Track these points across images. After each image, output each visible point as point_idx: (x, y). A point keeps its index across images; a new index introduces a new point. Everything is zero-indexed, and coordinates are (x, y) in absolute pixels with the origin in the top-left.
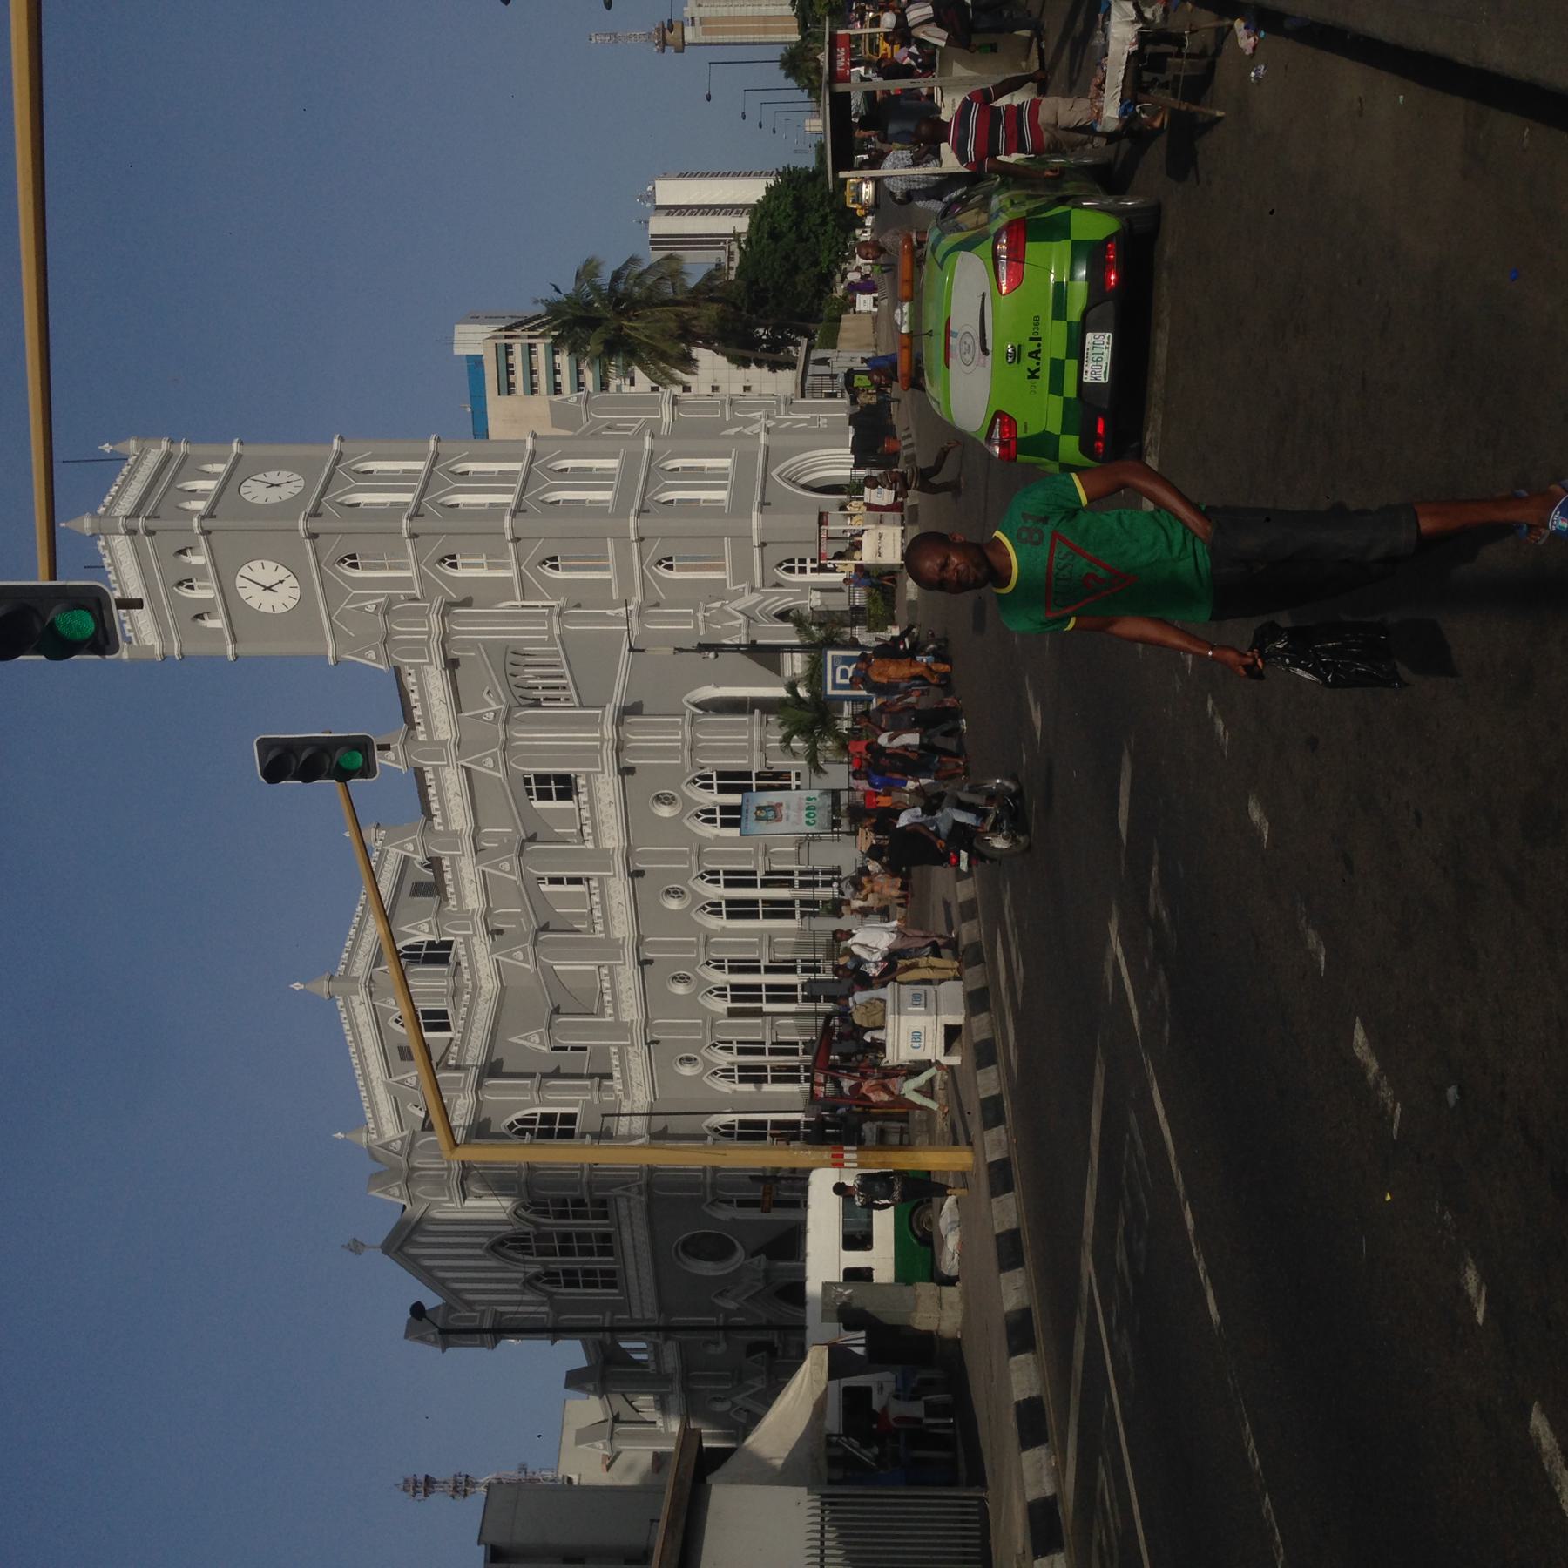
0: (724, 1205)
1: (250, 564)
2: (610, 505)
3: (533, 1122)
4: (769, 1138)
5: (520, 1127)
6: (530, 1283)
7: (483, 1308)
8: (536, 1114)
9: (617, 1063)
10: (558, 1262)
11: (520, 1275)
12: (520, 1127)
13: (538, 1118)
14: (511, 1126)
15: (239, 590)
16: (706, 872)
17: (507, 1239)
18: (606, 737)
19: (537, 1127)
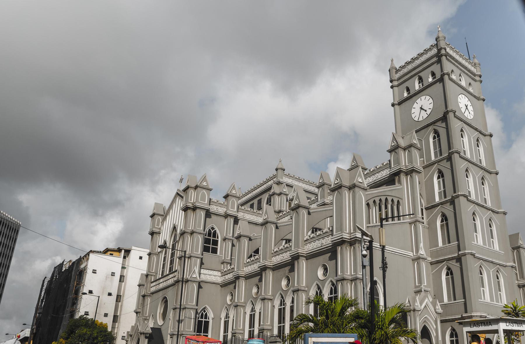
1: (431, 98)
2: (476, 243)
5: (212, 232)
7: (162, 229)
8: (218, 238)
12: (212, 232)
13: (216, 239)
14: (213, 228)
15: (420, 99)
18: (352, 235)
19: (212, 238)
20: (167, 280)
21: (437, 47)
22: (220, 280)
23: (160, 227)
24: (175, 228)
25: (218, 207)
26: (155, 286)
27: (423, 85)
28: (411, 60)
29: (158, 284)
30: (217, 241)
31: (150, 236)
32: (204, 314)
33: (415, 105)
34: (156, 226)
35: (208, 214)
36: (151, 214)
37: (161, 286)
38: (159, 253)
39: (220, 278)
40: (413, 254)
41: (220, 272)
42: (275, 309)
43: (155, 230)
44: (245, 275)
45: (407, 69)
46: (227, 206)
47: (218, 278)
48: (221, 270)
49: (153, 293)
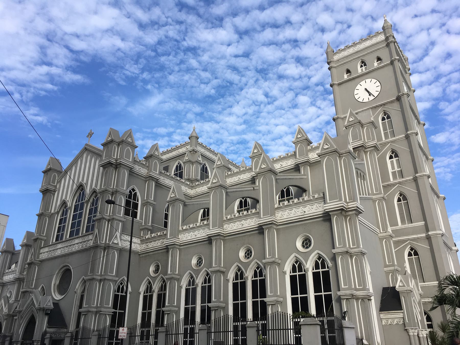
0: (83, 288)
3: (134, 199)
4: (114, 310)
5: (133, 193)
6: (64, 203)
7: (58, 187)
8: (138, 201)
9: (159, 235)
10: (71, 213)
11: (68, 199)
12: (133, 193)
13: (136, 202)
14: (133, 190)
16: (261, 269)
17: (84, 191)
20: (70, 246)
21: (385, 35)
22: (140, 248)
23: (55, 185)
24: (81, 187)
25: (140, 167)
26: (47, 252)
27: (366, 69)
28: (353, 44)
29: (54, 250)
30: (137, 205)
31: (41, 195)
32: (121, 287)
33: (358, 87)
34: (51, 184)
35: (132, 172)
36: (44, 169)
37: (58, 253)
38: (52, 214)
39: (139, 246)
40: (380, 231)
41: (139, 239)
42: (229, 284)
43: (50, 187)
44: (181, 244)
45: (348, 52)
46: (148, 168)
47: (138, 245)
48: (141, 237)
49: (42, 261)
